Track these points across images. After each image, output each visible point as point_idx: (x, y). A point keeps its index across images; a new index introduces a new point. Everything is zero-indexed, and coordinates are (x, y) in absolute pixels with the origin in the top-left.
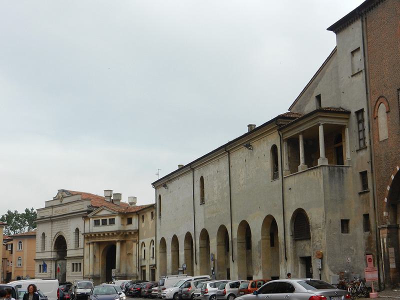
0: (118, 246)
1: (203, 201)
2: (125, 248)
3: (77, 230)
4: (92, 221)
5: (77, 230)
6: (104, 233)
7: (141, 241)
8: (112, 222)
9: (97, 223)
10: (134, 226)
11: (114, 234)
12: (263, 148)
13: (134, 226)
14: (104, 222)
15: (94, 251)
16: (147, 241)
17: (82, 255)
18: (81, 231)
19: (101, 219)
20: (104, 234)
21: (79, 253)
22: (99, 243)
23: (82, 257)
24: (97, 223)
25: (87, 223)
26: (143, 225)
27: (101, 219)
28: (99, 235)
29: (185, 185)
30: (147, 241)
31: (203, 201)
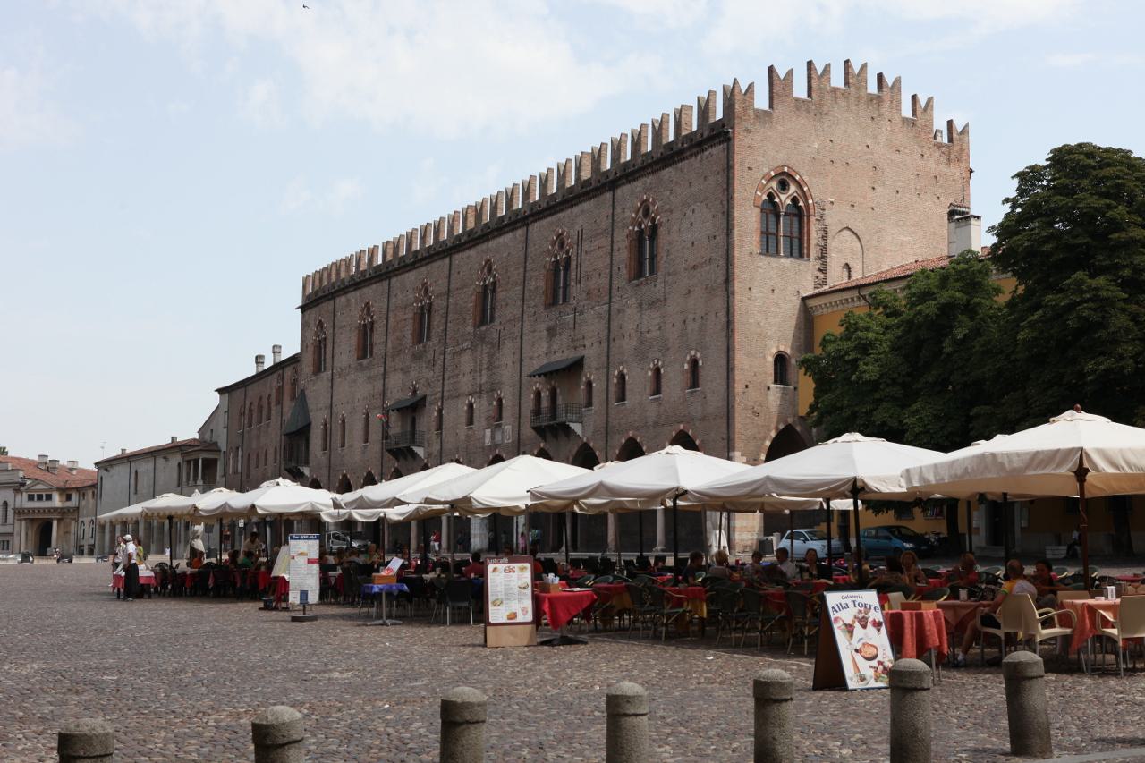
0: (55, 524)
1: (136, 493)
2: (62, 525)
3: (5, 503)
4: (25, 495)
5: (5, 503)
6: (39, 510)
7: (80, 519)
8: (49, 497)
9: (31, 498)
10: (74, 502)
11: (50, 510)
12: (176, 459)
13: (74, 502)
14: (40, 498)
15: (27, 528)
16: (87, 520)
17: (11, 531)
18: (11, 505)
19: (36, 494)
20: (39, 510)
21: (8, 529)
22: (32, 520)
23: (12, 534)
24: (31, 498)
25: (19, 497)
26: (83, 503)
27: (36, 494)
28: (33, 510)
29: (121, 471)
30: (87, 520)
31: (136, 493)
